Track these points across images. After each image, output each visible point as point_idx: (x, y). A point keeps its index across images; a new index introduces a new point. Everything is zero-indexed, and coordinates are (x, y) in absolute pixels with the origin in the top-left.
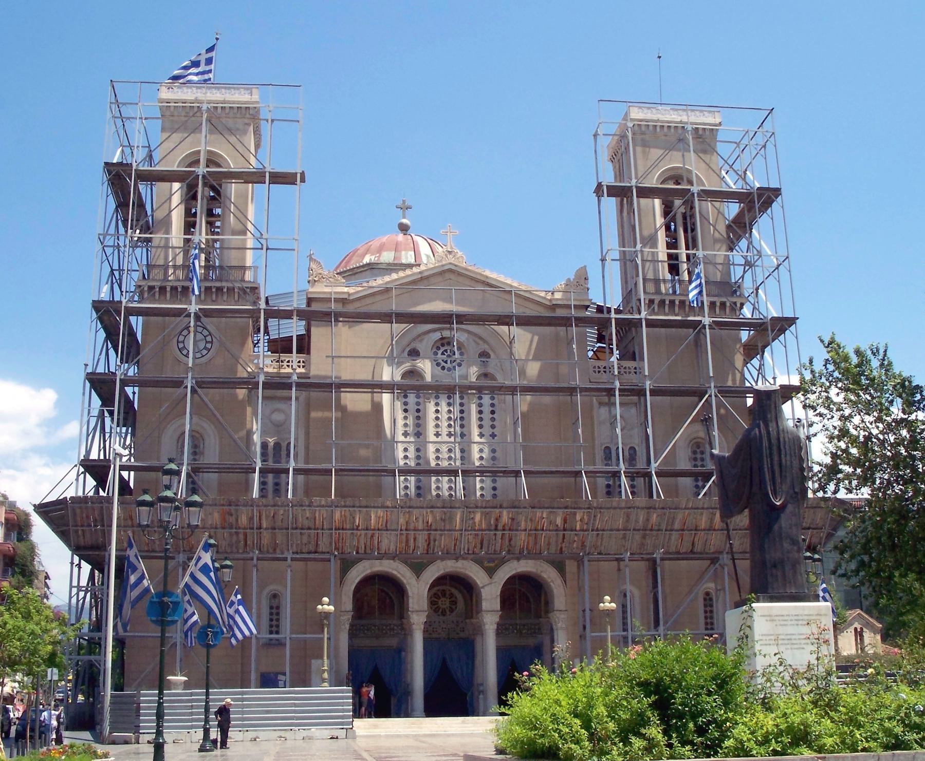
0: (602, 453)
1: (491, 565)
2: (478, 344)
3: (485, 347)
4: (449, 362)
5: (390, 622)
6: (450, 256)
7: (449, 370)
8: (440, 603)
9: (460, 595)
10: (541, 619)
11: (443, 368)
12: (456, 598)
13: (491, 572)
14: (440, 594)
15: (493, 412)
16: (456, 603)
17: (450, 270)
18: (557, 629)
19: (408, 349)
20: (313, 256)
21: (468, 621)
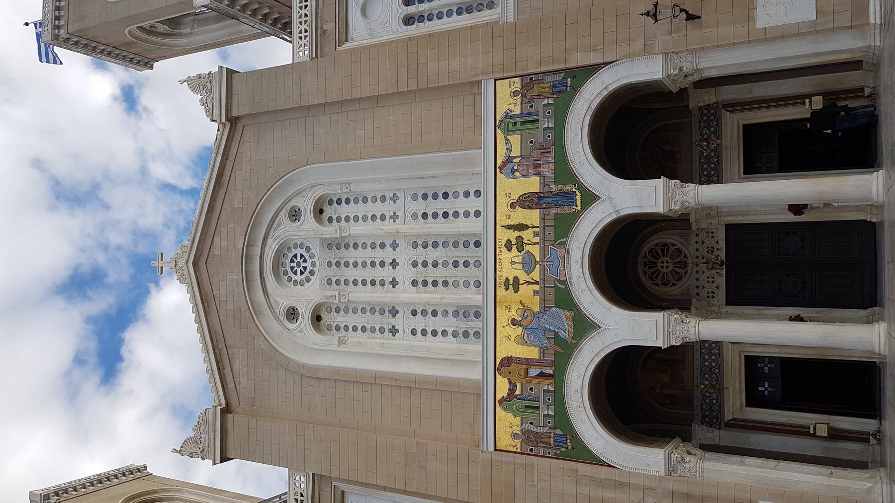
0: (414, 27)
1: (578, 198)
2: (279, 225)
3: (284, 214)
4: (304, 264)
5: (697, 355)
6: (180, 264)
7: (313, 264)
8: (665, 270)
9: (652, 238)
10: (690, 107)
11: (312, 273)
12: (657, 245)
13: (590, 198)
14: (653, 270)
15: (365, 200)
16: (665, 245)
17: (195, 264)
18: (698, 70)
19: (286, 323)
20: (178, 449)
21: (694, 227)
